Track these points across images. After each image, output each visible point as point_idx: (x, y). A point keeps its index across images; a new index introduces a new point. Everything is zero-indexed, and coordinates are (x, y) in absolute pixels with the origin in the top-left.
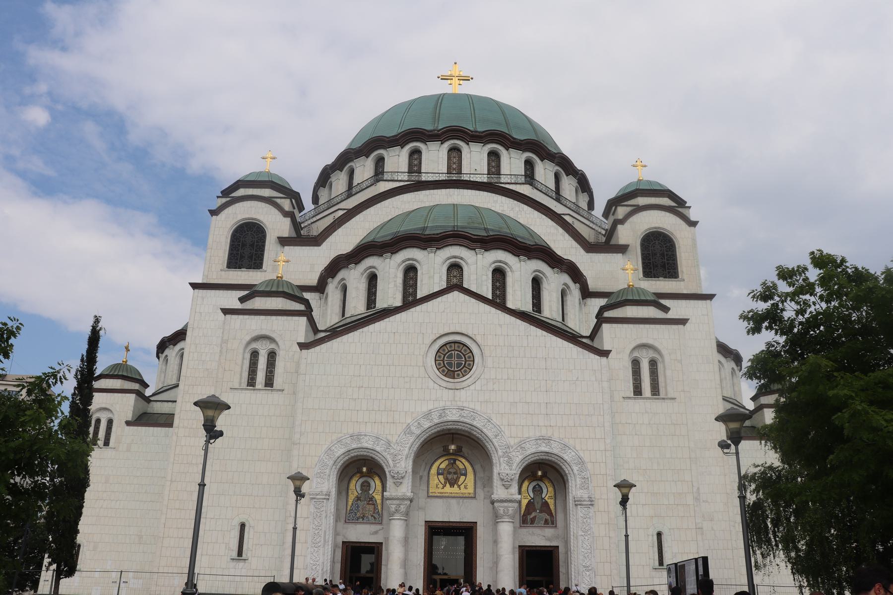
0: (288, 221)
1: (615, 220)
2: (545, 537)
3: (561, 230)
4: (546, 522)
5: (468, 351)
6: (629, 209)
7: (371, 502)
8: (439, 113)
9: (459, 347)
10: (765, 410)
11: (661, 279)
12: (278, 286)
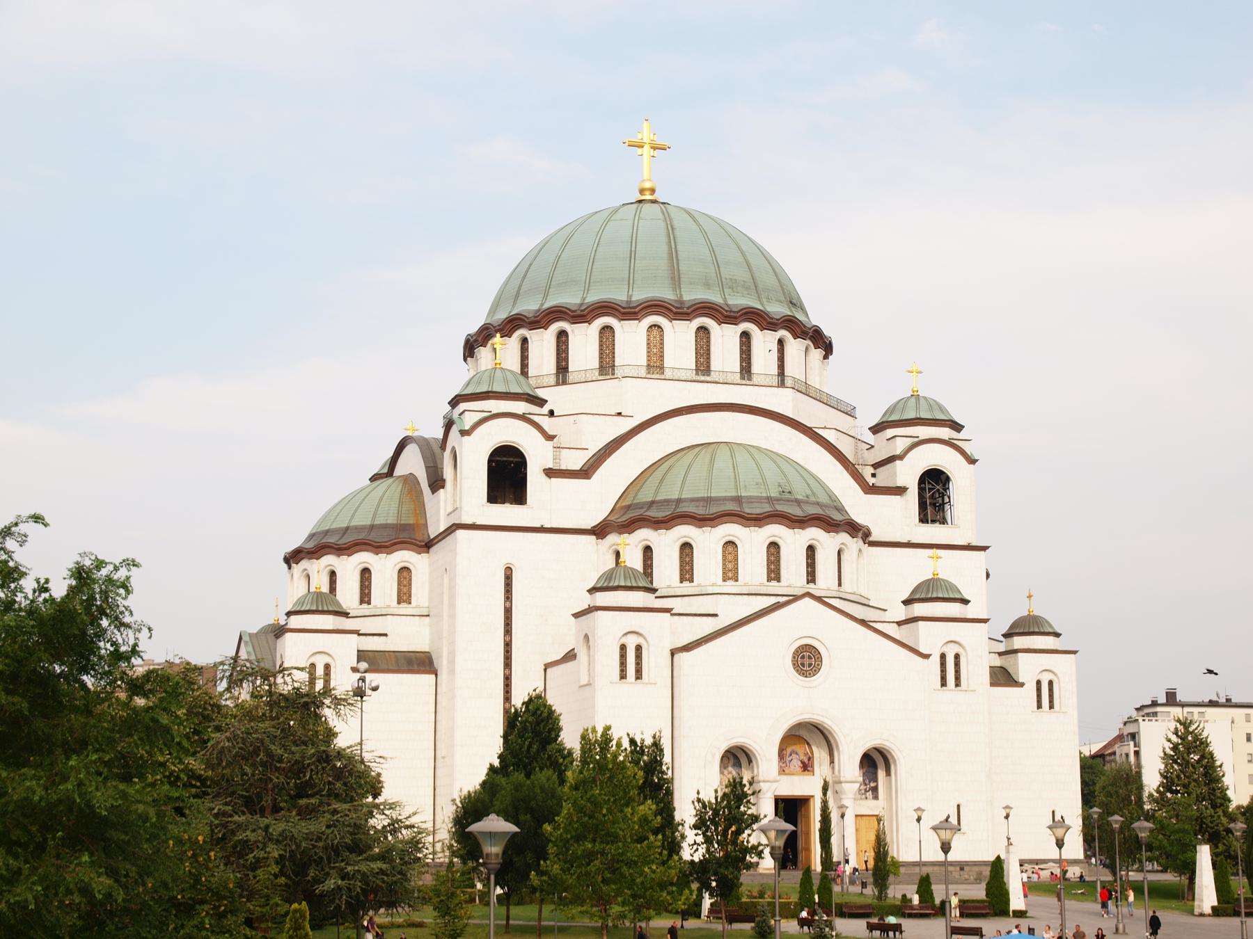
5: (817, 653)
6: (909, 441)
8: (679, 270)
9: (809, 649)
10: (1020, 654)
11: (937, 525)
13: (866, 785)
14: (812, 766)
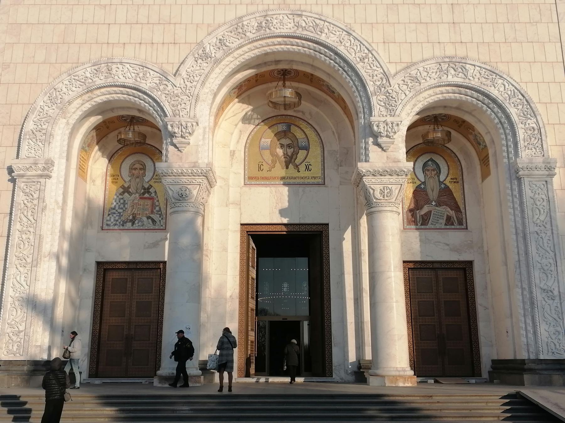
2: (448, 245)
4: (449, 221)
7: (146, 195)
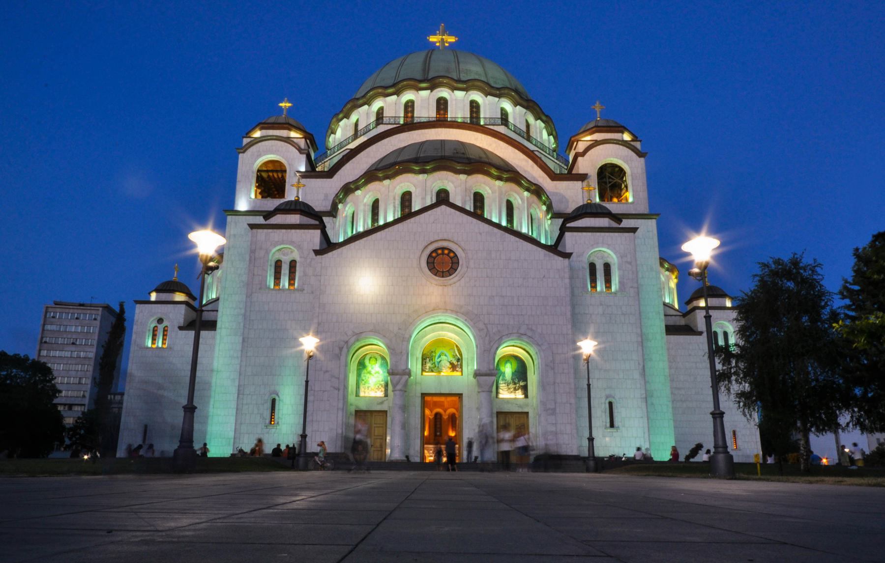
0: (303, 158)
1: (576, 153)
3: (530, 162)
12: (296, 205)
13: (515, 384)
14: (461, 367)
